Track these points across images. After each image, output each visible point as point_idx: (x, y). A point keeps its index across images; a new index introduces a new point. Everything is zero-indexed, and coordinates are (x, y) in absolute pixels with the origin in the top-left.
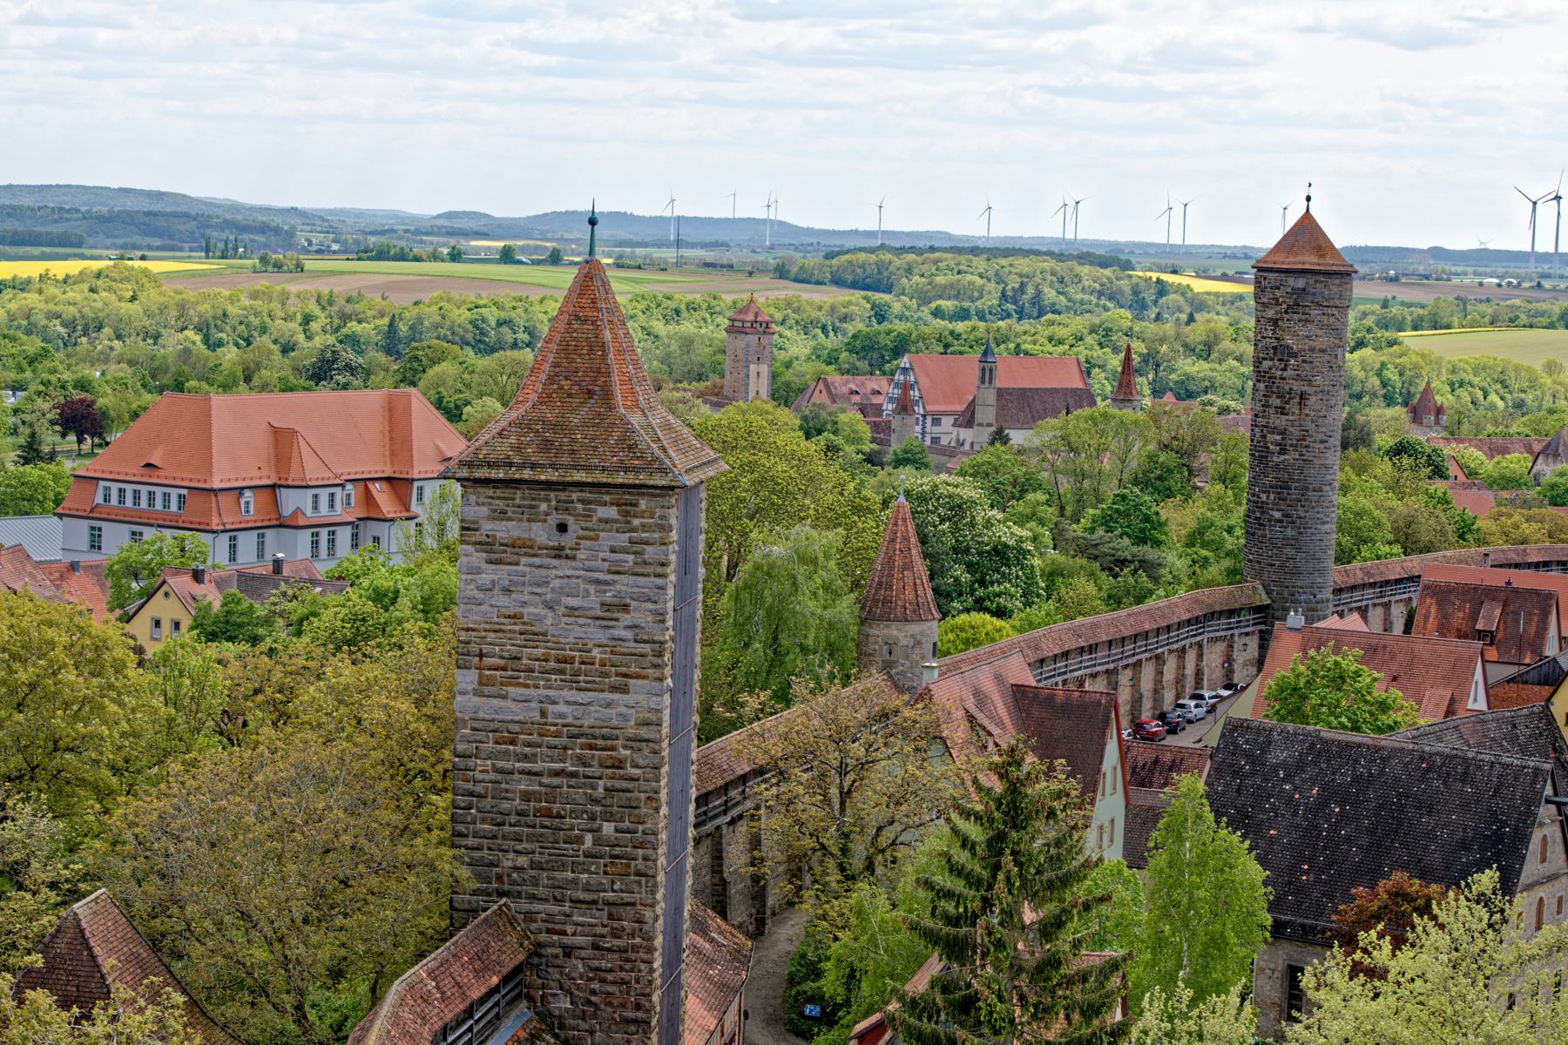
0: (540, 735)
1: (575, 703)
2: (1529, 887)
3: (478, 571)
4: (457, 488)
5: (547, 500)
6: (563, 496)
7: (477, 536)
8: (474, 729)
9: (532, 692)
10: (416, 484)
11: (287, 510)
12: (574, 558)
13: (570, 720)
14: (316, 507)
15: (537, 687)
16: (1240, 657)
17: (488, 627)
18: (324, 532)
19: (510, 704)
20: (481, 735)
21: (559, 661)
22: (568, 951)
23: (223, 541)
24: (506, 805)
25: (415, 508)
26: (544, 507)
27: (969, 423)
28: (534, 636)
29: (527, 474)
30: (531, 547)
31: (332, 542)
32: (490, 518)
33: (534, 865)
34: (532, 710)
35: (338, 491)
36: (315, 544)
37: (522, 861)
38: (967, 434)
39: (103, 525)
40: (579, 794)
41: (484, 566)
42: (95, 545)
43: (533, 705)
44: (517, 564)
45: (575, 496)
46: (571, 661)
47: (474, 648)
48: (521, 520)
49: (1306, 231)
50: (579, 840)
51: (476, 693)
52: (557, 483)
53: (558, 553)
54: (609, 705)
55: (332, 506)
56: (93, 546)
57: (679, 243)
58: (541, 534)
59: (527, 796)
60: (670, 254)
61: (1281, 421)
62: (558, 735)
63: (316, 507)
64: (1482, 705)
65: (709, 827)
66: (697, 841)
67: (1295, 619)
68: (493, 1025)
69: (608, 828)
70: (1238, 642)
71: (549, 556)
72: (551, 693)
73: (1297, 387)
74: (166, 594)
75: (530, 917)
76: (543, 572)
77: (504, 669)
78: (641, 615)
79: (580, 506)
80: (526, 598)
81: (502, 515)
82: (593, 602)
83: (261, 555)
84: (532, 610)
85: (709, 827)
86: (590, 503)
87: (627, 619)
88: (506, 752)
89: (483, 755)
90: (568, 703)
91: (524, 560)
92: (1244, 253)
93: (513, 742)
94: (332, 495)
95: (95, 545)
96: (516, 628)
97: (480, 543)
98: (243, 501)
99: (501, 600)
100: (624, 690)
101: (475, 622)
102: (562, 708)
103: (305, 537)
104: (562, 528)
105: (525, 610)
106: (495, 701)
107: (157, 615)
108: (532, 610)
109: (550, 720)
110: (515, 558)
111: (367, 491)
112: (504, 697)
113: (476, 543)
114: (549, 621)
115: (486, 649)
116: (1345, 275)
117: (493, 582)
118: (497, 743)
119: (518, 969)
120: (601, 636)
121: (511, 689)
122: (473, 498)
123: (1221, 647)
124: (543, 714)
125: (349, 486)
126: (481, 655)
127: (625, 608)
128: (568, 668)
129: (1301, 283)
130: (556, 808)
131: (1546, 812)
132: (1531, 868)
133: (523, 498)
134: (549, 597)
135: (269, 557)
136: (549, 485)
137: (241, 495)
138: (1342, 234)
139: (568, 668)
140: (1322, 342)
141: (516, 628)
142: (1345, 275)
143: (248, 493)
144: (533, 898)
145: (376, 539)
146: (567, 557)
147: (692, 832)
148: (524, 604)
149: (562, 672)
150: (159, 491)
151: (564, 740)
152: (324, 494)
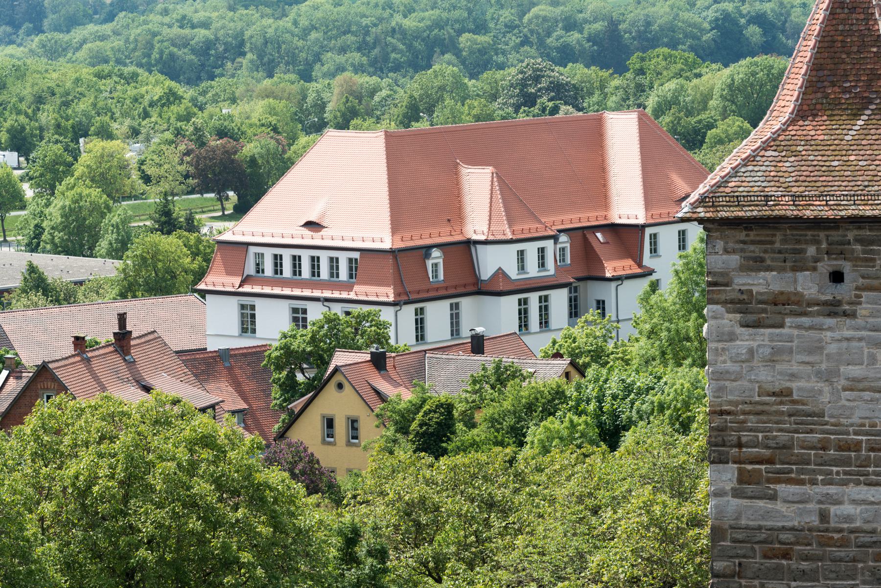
0: (821, 544)
1: (864, 502)
3: (732, 337)
4: (695, 232)
5: (817, 242)
6: (835, 235)
7: (730, 293)
8: (735, 541)
9: (807, 488)
10: (648, 231)
11: (486, 272)
12: (853, 315)
13: (858, 524)
14: (522, 267)
15: (813, 482)
17: (747, 408)
18: (534, 298)
19: (779, 506)
20: (742, 549)
21: (840, 448)
23: (408, 313)
25: (648, 261)
26: (811, 251)
28: (808, 417)
29: (791, 212)
30: (797, 303)
31: (544, 310)
32: (743, 268)
34: (810, 512)
35: (549, 244)
36: (523, 314)
39: (258, 302)
41: (739, 330)
42: (248, 323)
43: (810, 506)
44: (781, 326)
45: (851, 235)
46: (857, 446)
47: (733, 436)
48: (781, 270)
51: (737, 494)
52: (828, 220)
53: (833, 308)
55: (542, 264)
56: (244, 330)
58: (808, 285)
62: (844, 543)
63: (522, 267)
71: (819, 314)
72: (832, 490)
74: (340, 386)
76: (811, 333)
77: (770, 461)
79: (859, 247)
80: (795, 368)
81: (756, 264)
83: (455, 330)
84: (802, 384)
86: (872, 243)
88: (778, 568)
89: (749, 574)
90: (854, 502)
91: (788, 321)
93: (786, 555)
94: (542, 251)
95: (248, 323)
96: (784, 408)
97: (732, 302)
98: (429, 263)
101: (730, 403)
102: (848, 509)
103: (509, 305)
104: (837, 277)
105: (794, 385)
106: (761, 503)
107: (328, 412)
108: (802, 384)
109: (832, 525)
110: (778, 319)
111: (586, 241)
112: (773, 497)
113: (724, 303)
114: (826, 398)
115: (746, 436)
117: (751, 352)
118: (765, 557)
121: (781, 488)
122: (720, 245)
124: (824, 516)
125: (563, 238)
126: (740, 445)
133: (784, 241)
134: (824, 366)
135: (466, 333)
136: (818, 223)
137: (428, 256)
141: (784, 408)
143: (436, 253)
145: (601, 305)
146: (845, 314)
148: (793, 376)
149: (846, 462)
150: (324, 256)
151: (853, 551)
152: (531, 249)
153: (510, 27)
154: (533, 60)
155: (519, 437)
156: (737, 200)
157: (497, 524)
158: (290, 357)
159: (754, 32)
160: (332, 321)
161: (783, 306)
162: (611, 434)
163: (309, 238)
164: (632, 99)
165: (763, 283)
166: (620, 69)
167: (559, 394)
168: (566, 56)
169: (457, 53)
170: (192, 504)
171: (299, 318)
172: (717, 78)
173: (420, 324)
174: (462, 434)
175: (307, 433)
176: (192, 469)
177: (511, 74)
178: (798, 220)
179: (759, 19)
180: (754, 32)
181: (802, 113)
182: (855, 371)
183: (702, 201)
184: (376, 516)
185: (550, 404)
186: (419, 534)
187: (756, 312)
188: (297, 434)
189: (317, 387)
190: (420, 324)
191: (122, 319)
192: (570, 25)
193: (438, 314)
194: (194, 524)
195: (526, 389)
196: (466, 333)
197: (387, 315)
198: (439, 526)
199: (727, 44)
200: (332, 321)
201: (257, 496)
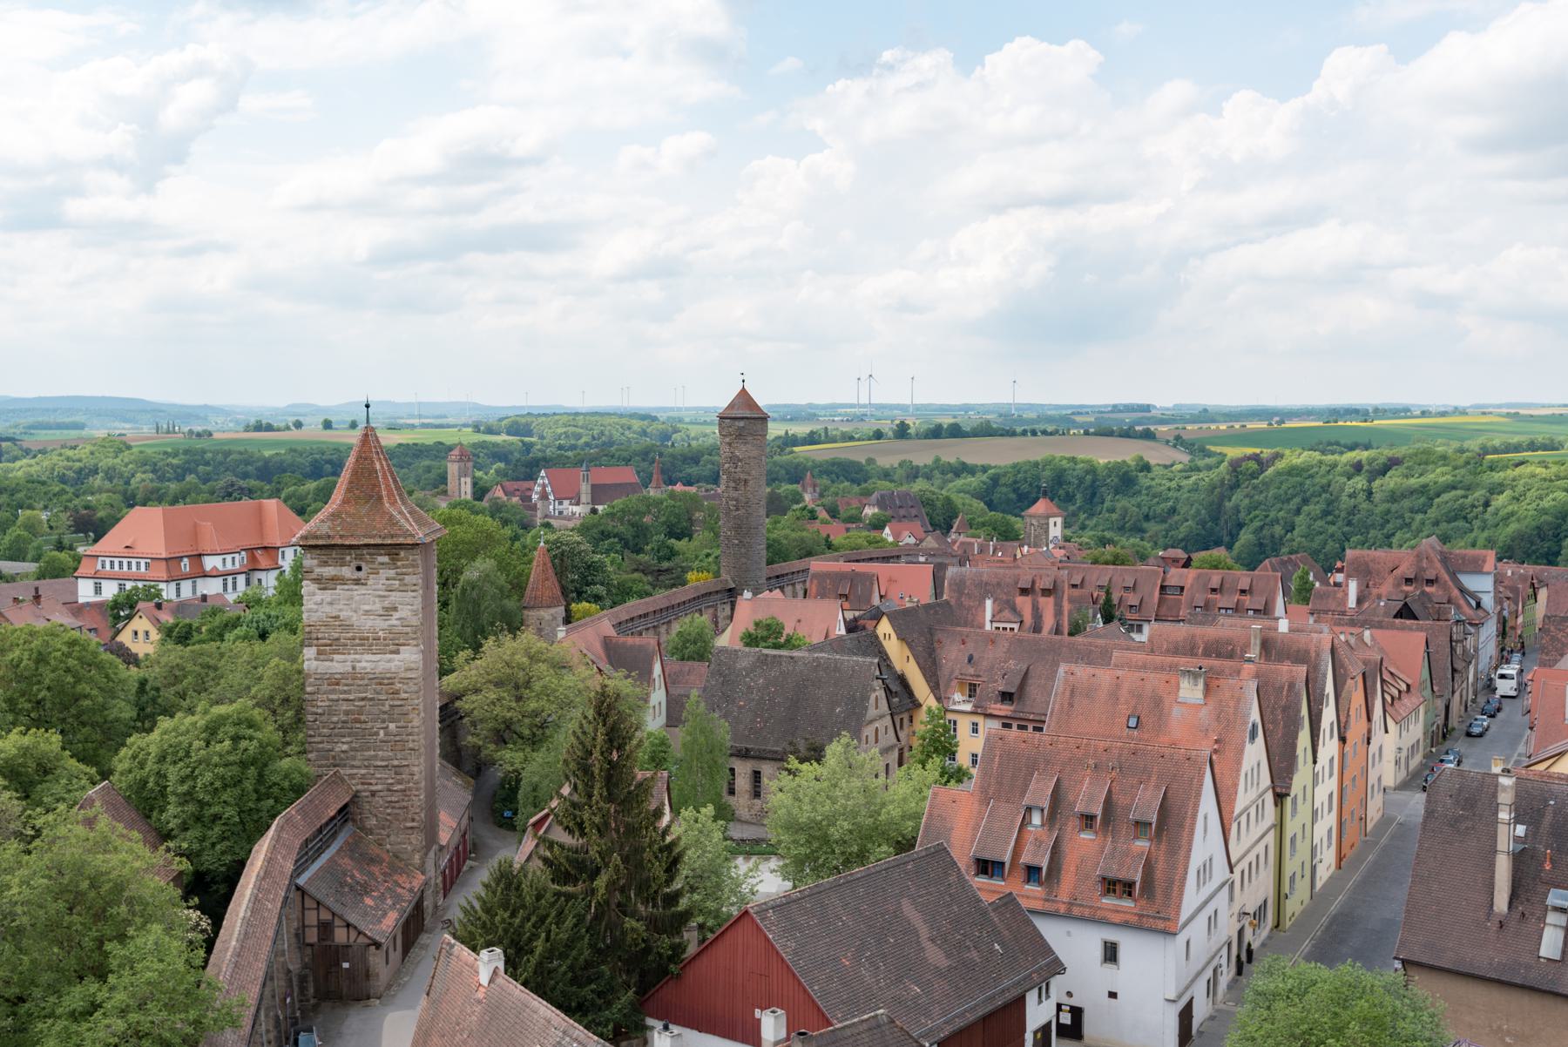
2: (871, 722)
7: (313, 576)
16: (721, 615)
18: (230, 579)
22: (373, 794)
23: (173, 586)
24: (335, 719)
25: (280, 562)
27: (578, 504)
28: (347, 627)
29: (339, 542)
31: (235, 584)
33: (353, 749)
36: (225, 585)
37: (345, 747)
38: (577, 509)
40: (375, 710)
42: (98, 590)
49: (744, 397)
50: (377, 734)
53: (357, 582)
54: (389, 661)
57: (420, 417)
59: (347, 713)
60: (416, 422)
61: (735, 494)
64: (843, 632)
65: (448, 721)
66: (441, 730)
67: (747, 595)
68: (334, 836)
69: (392, 726)
70: (720, 608)
73: (743, 476)
75: (352, 776)
78: (404, 612)
81: (325, 564)
82: (378, 606)
85: (448, 721)
87: (396, 615)
92: (715, 408)
95: (98, 590)
99: (328, 609)
100: (397, 652)
102: (364, 664)
104: (359, 569)
116: (764, 419)
119: (346, 806)
120: (385, 625)
123: (711, 611)
127: (395, 609)
128: (367, 642)
129: (742, 424)
130: (363, 718)
131: (877, 684)
132: (872, 712)
136: (351, 547)
138: (762, 400)
139: (367, 642)
140: (755, 453)
142: (764, 419)
144: (353, 767)
147: (438, 725)
150: (134, 562)
152: (229, 558)
153: (221, 463)
154: (230, 477)
155: (221, 637)
156: (316, 537)
157: (212, 675)
158: (116, 605)
159: (328, 467)
160: (136, 588)
161: (336, 581)
162: (263, 636)
163: (126, 552)
164: (275, 494)
165: (329, 571)
166: (270, 482)
167: (239, 618)
168: (245, 476)
169: (197, 474)
170: (68, 670)
171: (122, 587)
172: (311, 485)
173: (178, 590)
174: (196, 637)
175: (125, 637)
176: (68, 655)
177: (221, 483)
178: (342, 546)
179: (329, 462)
180: (328, 467)
181: (345, 501)
182: (367, 607)
183: (302, 538)
184: (154, 674)
185: (235, 623)
186: (177, 680)
187: (325, 583)
188: (119, 639)
189: (130, 617)
190: (178, 590)
191: (37, 589)
192: (247, 463)
193: (186, 587)
194: (70, 679)
195: (225, 617)
196: (199, 594)
197: (162, 586)
198: (185, 677)
199: (316, 472)
200: (136, 588)
201: (100, 666)
